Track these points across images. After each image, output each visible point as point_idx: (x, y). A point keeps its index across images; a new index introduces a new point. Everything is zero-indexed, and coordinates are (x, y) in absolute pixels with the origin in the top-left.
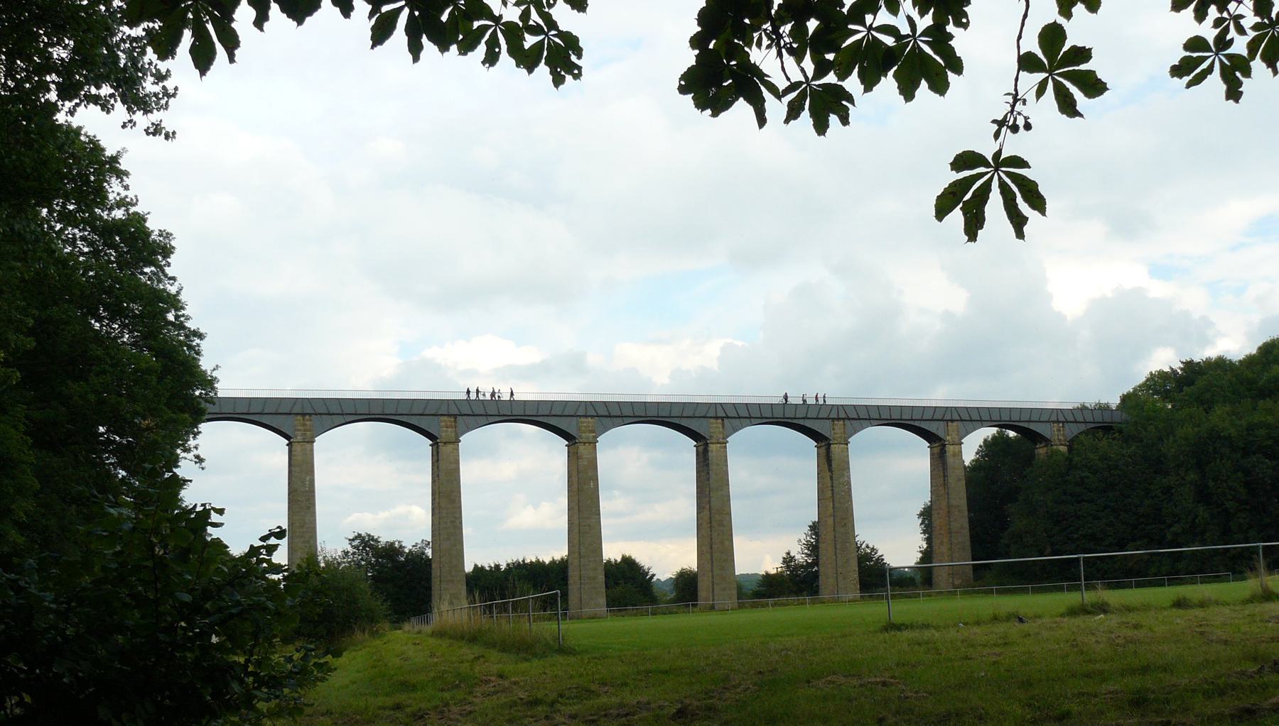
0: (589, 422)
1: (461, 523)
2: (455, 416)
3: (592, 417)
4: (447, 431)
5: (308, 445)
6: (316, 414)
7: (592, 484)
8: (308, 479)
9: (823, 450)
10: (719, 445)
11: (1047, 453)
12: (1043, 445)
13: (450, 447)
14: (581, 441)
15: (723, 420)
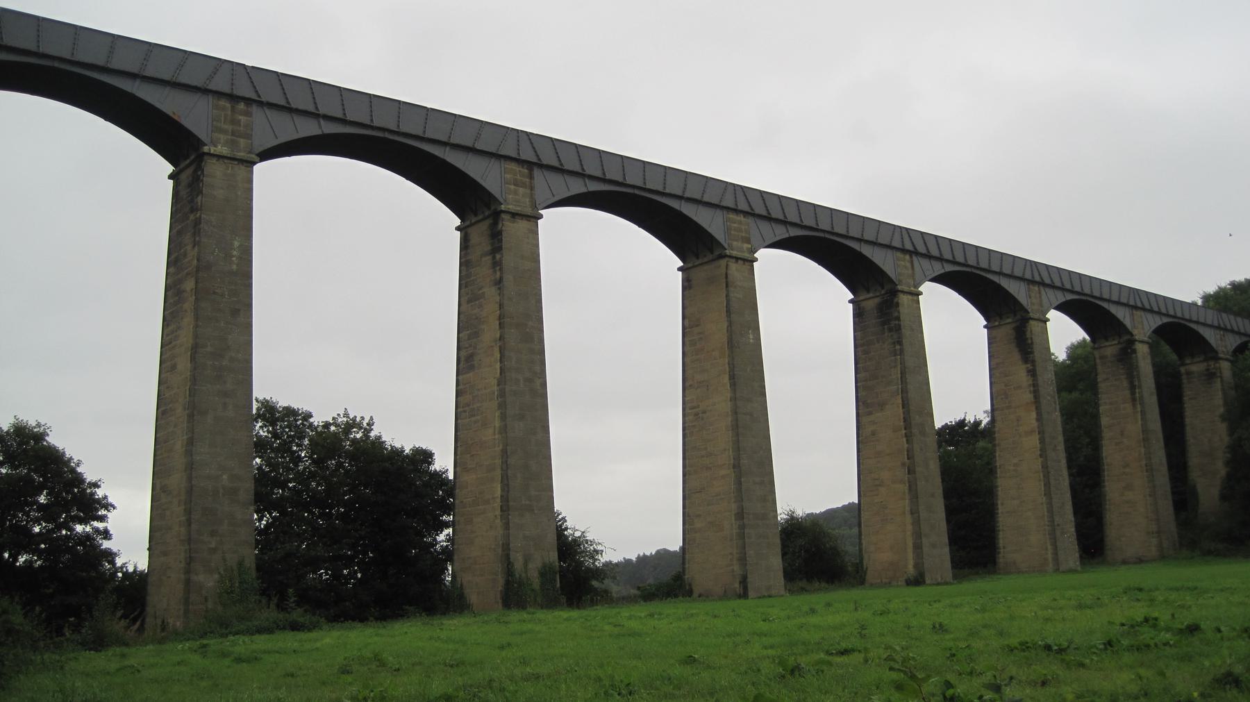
0: (740, 223)
1: (544, 385)
2: (530, 165)
3: (746, 213)
4: (516, 193)
5: (241, 170)
6: (261, 104)
7: (751, 337)
8: (236, 244)
9: (1007, 330)
10: (910, 297)
11: (1208, 370)
12: (1201, 359)
13: (522, 225)
14: (734, 253)
15: (911, 257)
